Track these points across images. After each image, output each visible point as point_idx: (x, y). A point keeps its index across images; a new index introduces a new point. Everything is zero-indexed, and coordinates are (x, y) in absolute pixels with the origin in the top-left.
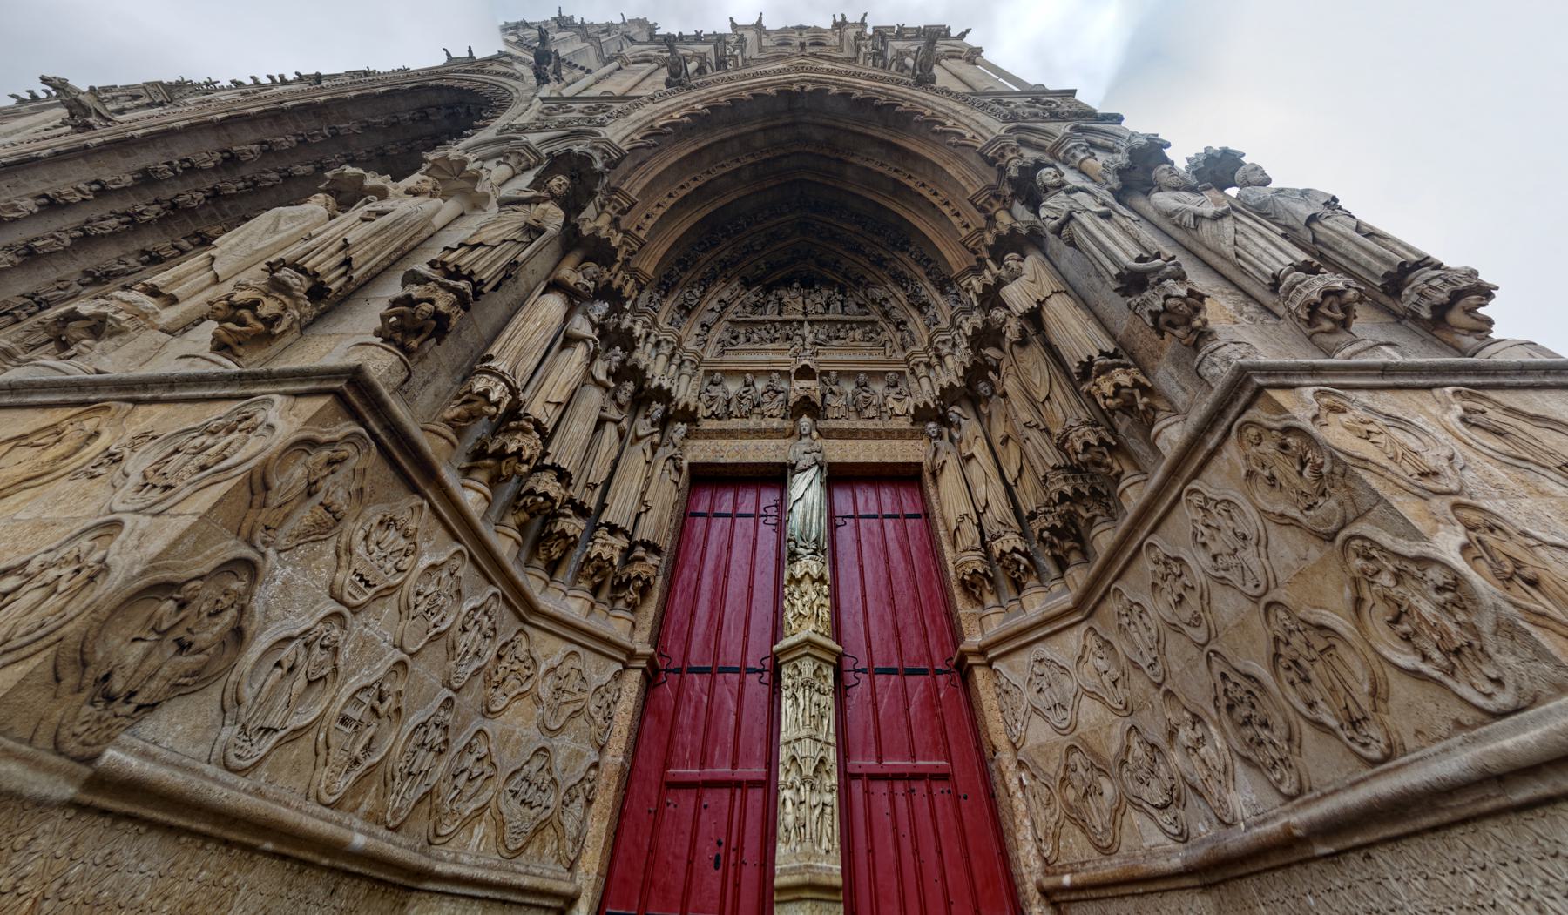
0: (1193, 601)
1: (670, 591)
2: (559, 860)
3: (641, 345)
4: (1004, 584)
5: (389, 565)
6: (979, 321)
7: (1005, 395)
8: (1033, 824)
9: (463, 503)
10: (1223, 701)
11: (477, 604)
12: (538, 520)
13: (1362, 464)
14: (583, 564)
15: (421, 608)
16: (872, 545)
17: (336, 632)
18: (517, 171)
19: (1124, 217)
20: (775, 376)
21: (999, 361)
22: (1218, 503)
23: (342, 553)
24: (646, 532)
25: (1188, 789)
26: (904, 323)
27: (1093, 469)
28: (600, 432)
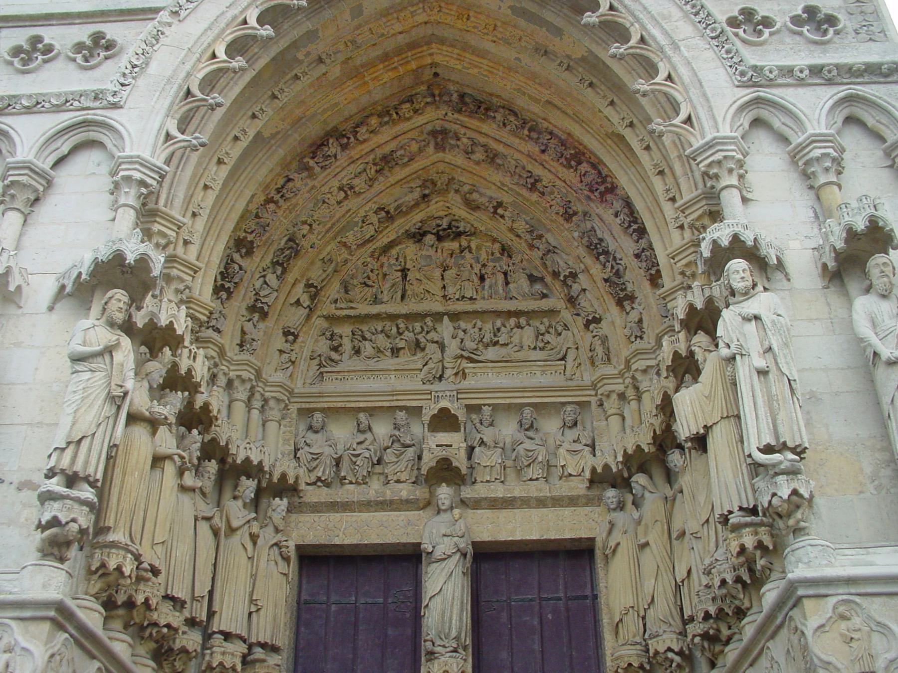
20: (401, 415)
24: (262, 632)
26: (597, 320)
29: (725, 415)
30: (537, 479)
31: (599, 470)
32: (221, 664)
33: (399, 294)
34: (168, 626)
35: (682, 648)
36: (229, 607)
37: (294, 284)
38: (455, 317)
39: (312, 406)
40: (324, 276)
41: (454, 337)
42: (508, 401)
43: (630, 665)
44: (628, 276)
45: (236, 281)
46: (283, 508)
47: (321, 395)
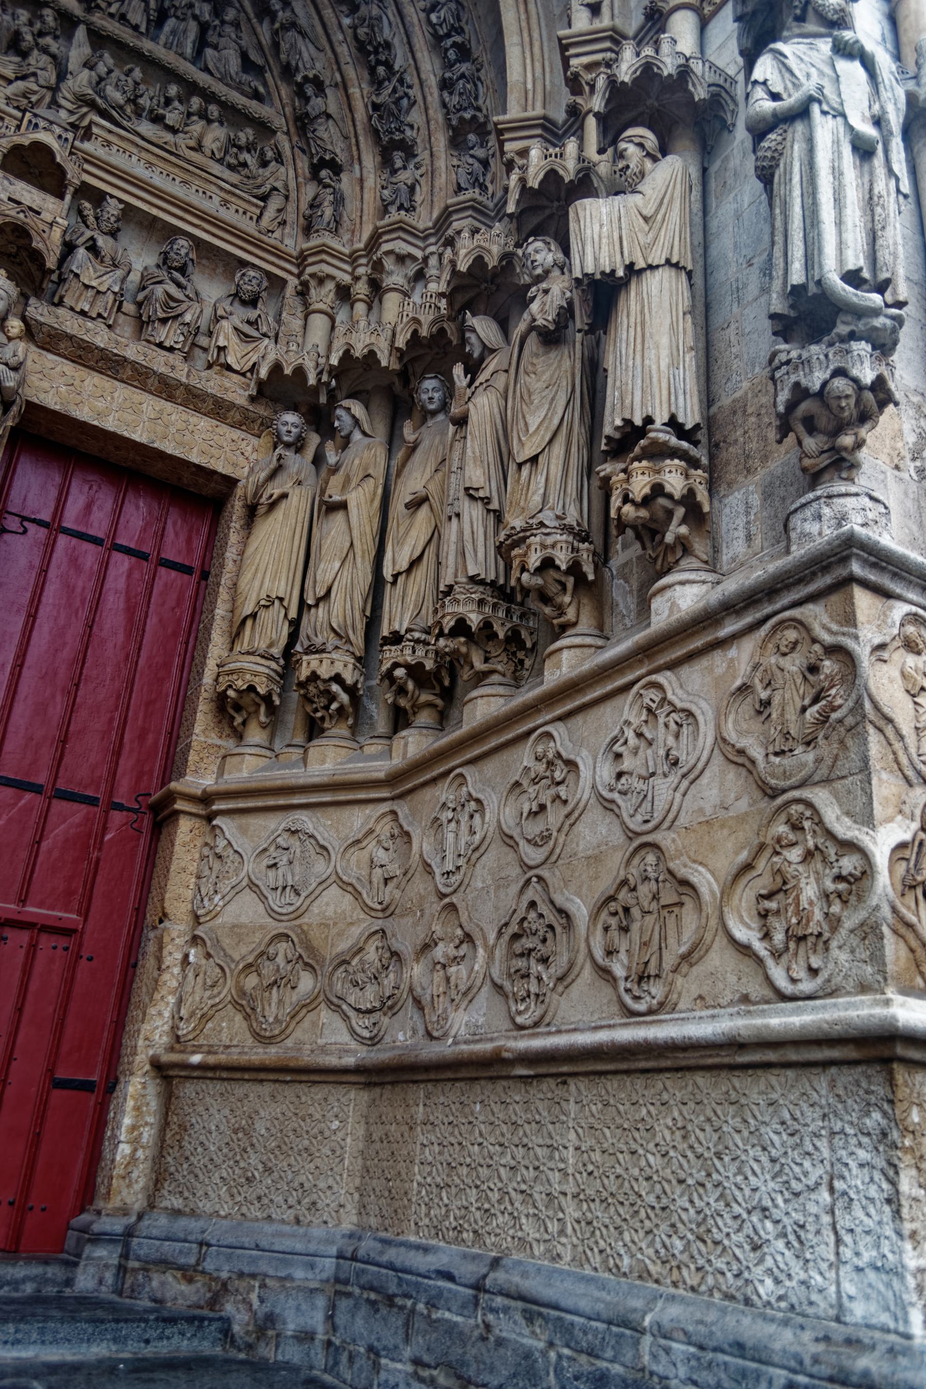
0: (554, 816)
4: (293, 720)
6: (495, 249)
7: (461, 422)
8: (180, 1002)
10: (514, 928)
13: (881, 723)
16: (68, 588)
19: (890, 172)
21: (488, 351)
22: (675, 710)
25: (410, 1000)
26: (336, 168)
27: (533, 604)
29: (674, 261)
30: (171, 349)
31: (288, 371)
35: (357, 682)
38: (98, 39)
41: (89, 65)
42: (154, 212)
43: (252, 688)
44: (415, 116)
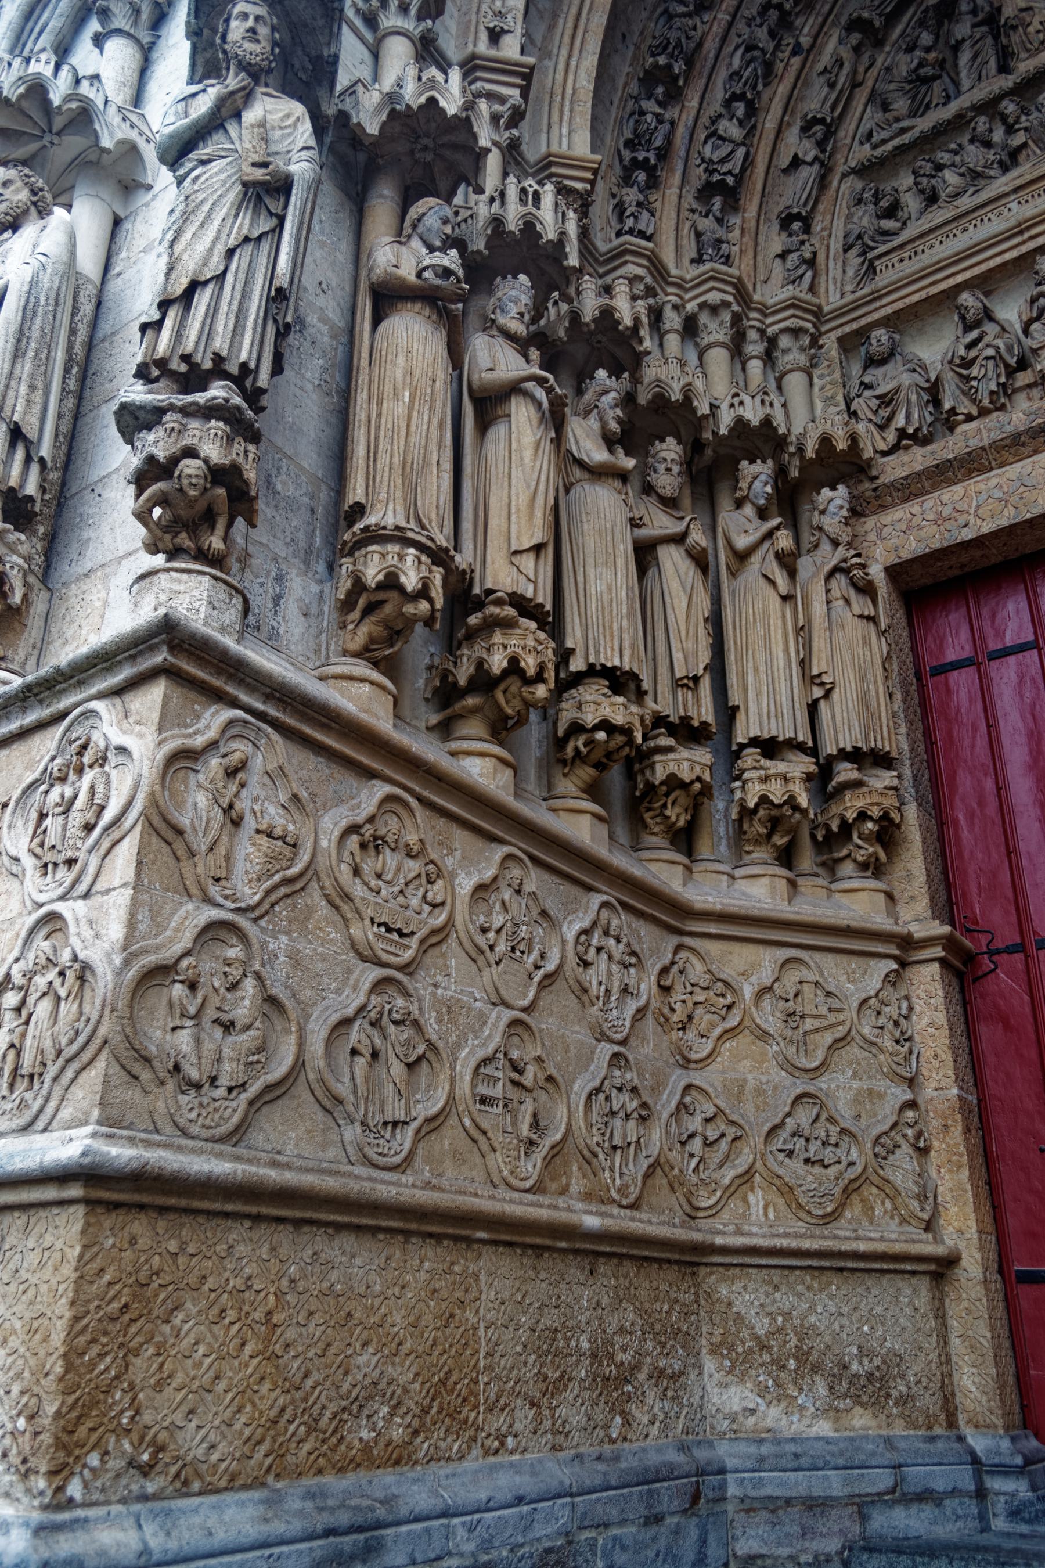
1: (941, 824)
2: (904, 1221)
3: (647, 344)
5: (415, 902)
9: (469, 781)
11: (586, 923)
12: (616, 774)
14: (740, 821)
15: (502, 947)
17: (400, 1002)
18: (146, 39)
23: (338, 901)
28: (652, 573)
32: (764, 799)
33: (993, 64)
34: (605, 725)
36: (758, 694)
37: (779, 132)
39: (863, 322)
40: (833, 96)
45: (658, 143)
46: (838, 502)
47: (876, 296)
